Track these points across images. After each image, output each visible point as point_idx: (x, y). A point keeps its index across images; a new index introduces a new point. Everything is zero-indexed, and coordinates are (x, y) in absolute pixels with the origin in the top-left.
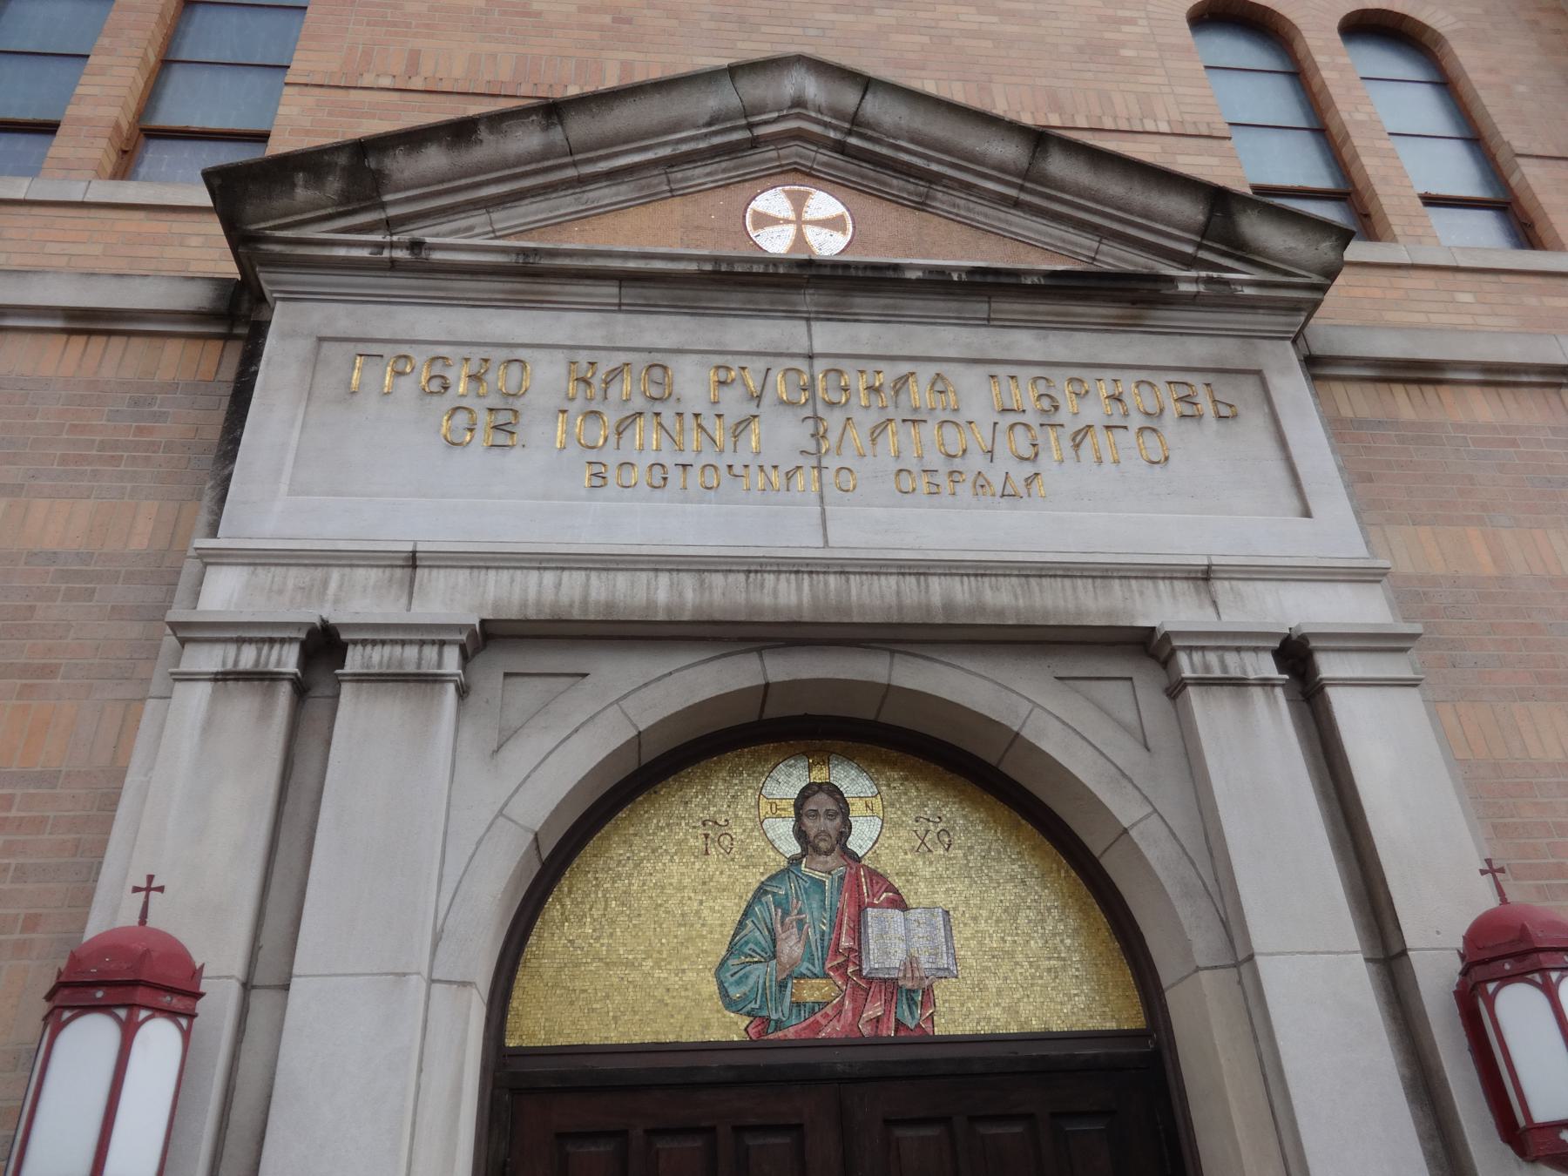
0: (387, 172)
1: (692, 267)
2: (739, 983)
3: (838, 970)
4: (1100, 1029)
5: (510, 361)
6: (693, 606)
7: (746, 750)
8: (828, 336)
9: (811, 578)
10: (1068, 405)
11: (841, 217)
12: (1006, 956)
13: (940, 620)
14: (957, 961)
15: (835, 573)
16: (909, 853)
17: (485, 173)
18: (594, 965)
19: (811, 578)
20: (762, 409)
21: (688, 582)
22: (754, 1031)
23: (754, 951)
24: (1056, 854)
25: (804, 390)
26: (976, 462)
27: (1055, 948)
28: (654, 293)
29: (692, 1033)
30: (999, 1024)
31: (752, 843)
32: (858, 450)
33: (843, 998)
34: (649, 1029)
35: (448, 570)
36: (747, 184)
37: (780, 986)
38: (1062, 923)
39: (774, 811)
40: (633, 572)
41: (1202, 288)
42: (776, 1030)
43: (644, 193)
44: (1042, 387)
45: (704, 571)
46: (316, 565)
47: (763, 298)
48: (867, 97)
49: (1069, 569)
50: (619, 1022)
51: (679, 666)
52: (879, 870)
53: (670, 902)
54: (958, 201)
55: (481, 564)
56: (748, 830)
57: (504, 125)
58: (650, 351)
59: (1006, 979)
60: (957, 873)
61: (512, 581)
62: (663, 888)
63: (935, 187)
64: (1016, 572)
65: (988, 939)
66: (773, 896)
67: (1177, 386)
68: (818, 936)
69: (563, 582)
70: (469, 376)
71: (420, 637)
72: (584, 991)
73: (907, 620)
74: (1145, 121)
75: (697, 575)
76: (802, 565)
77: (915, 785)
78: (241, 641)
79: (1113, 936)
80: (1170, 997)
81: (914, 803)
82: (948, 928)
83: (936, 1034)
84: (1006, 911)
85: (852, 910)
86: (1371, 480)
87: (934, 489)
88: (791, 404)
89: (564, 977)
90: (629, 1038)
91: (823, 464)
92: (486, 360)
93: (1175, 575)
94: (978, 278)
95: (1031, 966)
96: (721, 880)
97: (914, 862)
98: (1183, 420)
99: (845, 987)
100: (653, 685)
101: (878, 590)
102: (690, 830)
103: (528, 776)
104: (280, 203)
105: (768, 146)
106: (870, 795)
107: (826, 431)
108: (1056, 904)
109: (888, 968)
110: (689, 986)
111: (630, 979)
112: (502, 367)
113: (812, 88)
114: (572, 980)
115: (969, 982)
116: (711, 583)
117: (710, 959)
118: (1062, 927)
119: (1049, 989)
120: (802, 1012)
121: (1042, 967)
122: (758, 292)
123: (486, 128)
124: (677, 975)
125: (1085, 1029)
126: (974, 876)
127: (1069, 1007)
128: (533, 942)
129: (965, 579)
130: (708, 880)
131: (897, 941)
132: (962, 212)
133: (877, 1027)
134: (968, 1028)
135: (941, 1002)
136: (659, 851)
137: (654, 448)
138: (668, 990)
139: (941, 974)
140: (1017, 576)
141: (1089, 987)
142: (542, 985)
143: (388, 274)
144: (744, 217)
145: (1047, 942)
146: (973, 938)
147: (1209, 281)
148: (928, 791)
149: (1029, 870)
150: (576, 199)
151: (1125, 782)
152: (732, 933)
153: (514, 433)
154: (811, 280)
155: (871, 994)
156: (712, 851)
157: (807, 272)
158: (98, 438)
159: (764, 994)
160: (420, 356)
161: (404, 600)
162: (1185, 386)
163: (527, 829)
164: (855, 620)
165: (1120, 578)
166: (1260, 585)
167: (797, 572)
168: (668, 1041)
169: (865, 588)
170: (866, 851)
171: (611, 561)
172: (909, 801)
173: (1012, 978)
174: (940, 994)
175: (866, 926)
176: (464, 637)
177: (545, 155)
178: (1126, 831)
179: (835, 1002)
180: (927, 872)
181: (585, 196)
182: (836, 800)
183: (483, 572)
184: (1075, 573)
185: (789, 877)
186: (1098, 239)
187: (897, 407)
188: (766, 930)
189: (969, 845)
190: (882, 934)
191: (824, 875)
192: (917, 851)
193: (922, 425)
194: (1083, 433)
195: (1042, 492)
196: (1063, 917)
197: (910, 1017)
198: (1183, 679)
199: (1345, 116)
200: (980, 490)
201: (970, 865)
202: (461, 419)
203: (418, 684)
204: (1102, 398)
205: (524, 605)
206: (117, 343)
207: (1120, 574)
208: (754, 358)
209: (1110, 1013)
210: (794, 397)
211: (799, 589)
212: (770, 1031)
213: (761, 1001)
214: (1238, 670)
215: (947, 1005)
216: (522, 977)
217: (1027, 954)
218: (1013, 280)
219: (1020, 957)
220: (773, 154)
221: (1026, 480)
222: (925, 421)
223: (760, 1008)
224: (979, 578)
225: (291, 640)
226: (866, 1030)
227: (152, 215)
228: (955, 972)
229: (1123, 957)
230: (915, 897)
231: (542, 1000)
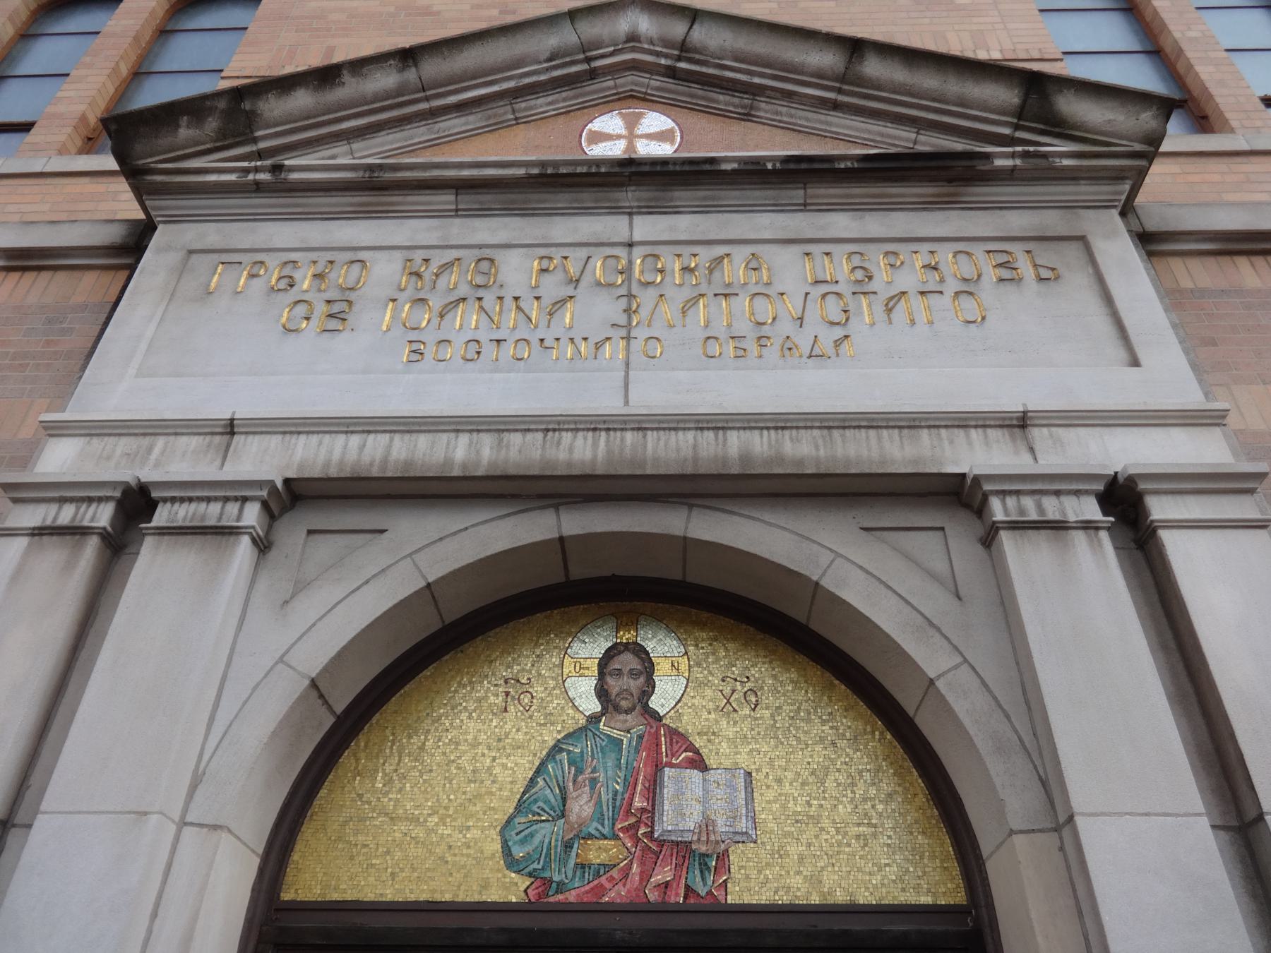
0: (259, 112)
1: (521, 172)
2: (523, 842)
3: (628, 831)
4: (913, 903)
5: (352, 262)
6: (489, 462)
7: (556, 612)
8: (647, 227)
9: (608, 435)
10: (882, 275)
11: (671, 131)
12: (811, 821)
13: (735, 470)
14: (757, 824)
15: (633, 429)
16: (713, 712)
17: (345, 110)
18: (380, 819)
19: (608, 435)
20: (578, 290)
21: (487, 440)
22: (534, 892)
23: (543, 810)
24: (871, 716)
25: (621, 273)
26: (786, 327)
27: (866, 814)
28: (487, 198)
29: (470, 893)
30: (799, 894)
31: (552, 701)
32: (669, 321)
33: (631, 861)
34: (425, 887)
35: (263, 436)
36: (586, 111)
37: (566, 847)
38: (874, 788)
39: (577, 670)
40: (435, 434)
41: (1018, 162)
42: (557, 892)
43: (491, 121)
44: (856, 261)
45: (503, 431)
46: (144, 435)
47: (587, 197)
48: (695, 27)
49: (873, 420)
50: (397, 879)
51: (476, 522)
52: (680, 730)
53: (463, 758)
54: (780, 109)
55: (293, 429)
56: (549, 689)
57: (365, 70)
58: (480, 247)
59: (809, 845)
60: (763, 733)
61: (320, 443)
62: (457, 744)
63: (758, 98)
64: (817, 424)
65: (792, 802)
66: (568, 754)
67: (995, 254)
68: (610, 795)
69: (368, 444)
70: (315, 276)
71: (222, 494)
72: (365, 846)
73: (702, 471)
74: (977, 51)
75: (496, 435)
76: (599, 422)
77: (724, 645)
78: (63, 500)
79: (931, 803)
80: (991, 867)
81: (722, 663)
82: (749, 789)
83: (729, 902)
84: (813, 773)
85: (649, 769)
86: (1215, 345)
87: (742, 353)
88: (611, 285)
89: (348, 831)
90: (404, 896)
91: (632, 335)
92: (331, 262)
93: (988, 423)
94: (792, 166)
95: (838, 832)
96: (517, 737)
97: (717, 722)
98: (1001, 284)
99: (634, 849)
100: (448, 539)
101: (674, 444)
102: (492, 688)
103: (314, 625)
104: (164, 141)
105: (605, 77)
106: (677, 655)
107: (638, 306)
108: (868, 767)
109: (682, 831)
110: (472, 844)
111: (413, 835)
112: (346, 267)
114: (356, 834)
115: (768, 847)
116: (509, 442)
117: (496, 817)
118: (874, 792)
119: (857, 857)
120: (587, 874)
121: (850, 834)
122: (582, 192)
123: (349, 72)
124: (461, 832)
125: (896, 903)
126: (780, 736)
127: (879, 877)
128: (323, 795)
129: (765, 432)
130: (503, 737)
131: (694, 802)
132: (785, 119)
133: (665, 893)
134: (764, 898)
135: (737, 868)
136: (459, 708)
137: (473, 327)
138: (450, 847)
139: (738, 838)
140: (819, 428)
141: (902, 857)
142: (325, 838)
143: (253, 195)
144: (581, 136)
145: (856, 807)
146: (775, 802)
147: (1026, 155)
148: (738, 651)
149: (841, 731)
150: (428, 129)
151: (932, 632)
152: (522, 790)
153: (345, 320)
154: (633, 178)
155: (661, 857)
156: (511, 708)
157: (627, 170)
158: (12, 350)
159: (548, 854)
160: (273, 261)
161: (218, 462)
162: (1005, 254)
163: (303, 675)
164: (649, 472)
165: (929, 427)
166: (1082, 431)
167: (595, 429)
168: (443, 900)
169: (662, 443)
170: (668, 710)
171: (413, 424)
172: (717, 661)
173: (817, 845)
174: (736, 860)
175: (662, 787)
176: (264, 493)
177: (399, 92)
178: (932, 682)
179: (622, 865)
180: (731, 732)
181: (437, 126)
182: (639, 657)
183: (295, 436)
184: (880, 424)
185: (586, 735)
186: (916, 130)
187: (710, 283)
188: (557, 788)
189: (777, 705)
190: (679, 793)
191: (622, 733)
192: (722, 710)
193: (733, 299)
194: (896, 298)
195: (852, 352)
196: (877, 780)
197: (701, 883)
198: (994, 523)
199: (1177, 35)
200: (787, 353)
201: (778, 725)
202: (301, 310)
203: (215, 536)
204: (918, 268)
205: (327, 464)
206: (45, 275)
207: (928, 424)
208: (577, 249)
209: (926, 886)
210: (611, 280)
211: (595, 444)
212: (550, 893)
213: (545, 862)
214: (1057, 513)
215: (743, 871)
216: (307, 831)
217: (834, 820)
218: (826, 166)
219: (826, 823)
220: (611, 83)
221: (836, 341)
222: (737, 295)
223: (543, 869)
224: (780, 431)
225: (108, 499)
226: (653, 896)
227: (95, 180)
228: (754, 836)
229: (942, 825)
230: (716, 757)
231: (323, 854)
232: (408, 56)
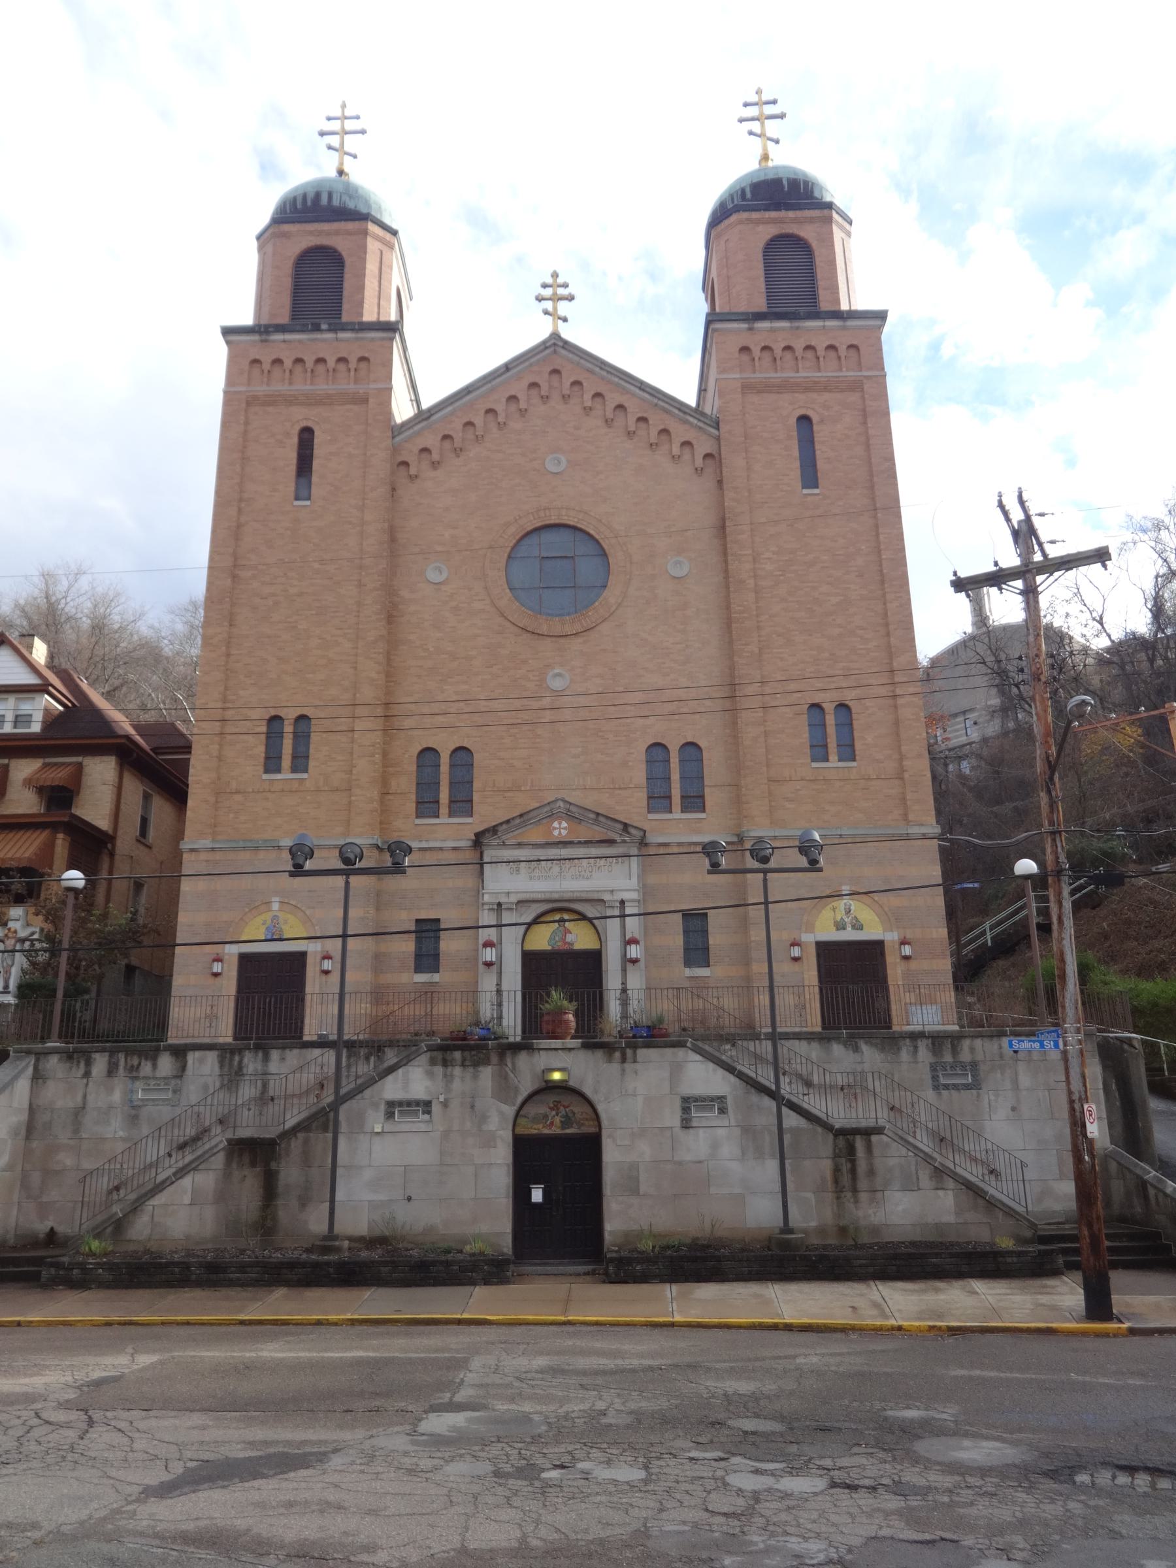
26: (583, 873)
113: (561, 804)
232: (521, 816)
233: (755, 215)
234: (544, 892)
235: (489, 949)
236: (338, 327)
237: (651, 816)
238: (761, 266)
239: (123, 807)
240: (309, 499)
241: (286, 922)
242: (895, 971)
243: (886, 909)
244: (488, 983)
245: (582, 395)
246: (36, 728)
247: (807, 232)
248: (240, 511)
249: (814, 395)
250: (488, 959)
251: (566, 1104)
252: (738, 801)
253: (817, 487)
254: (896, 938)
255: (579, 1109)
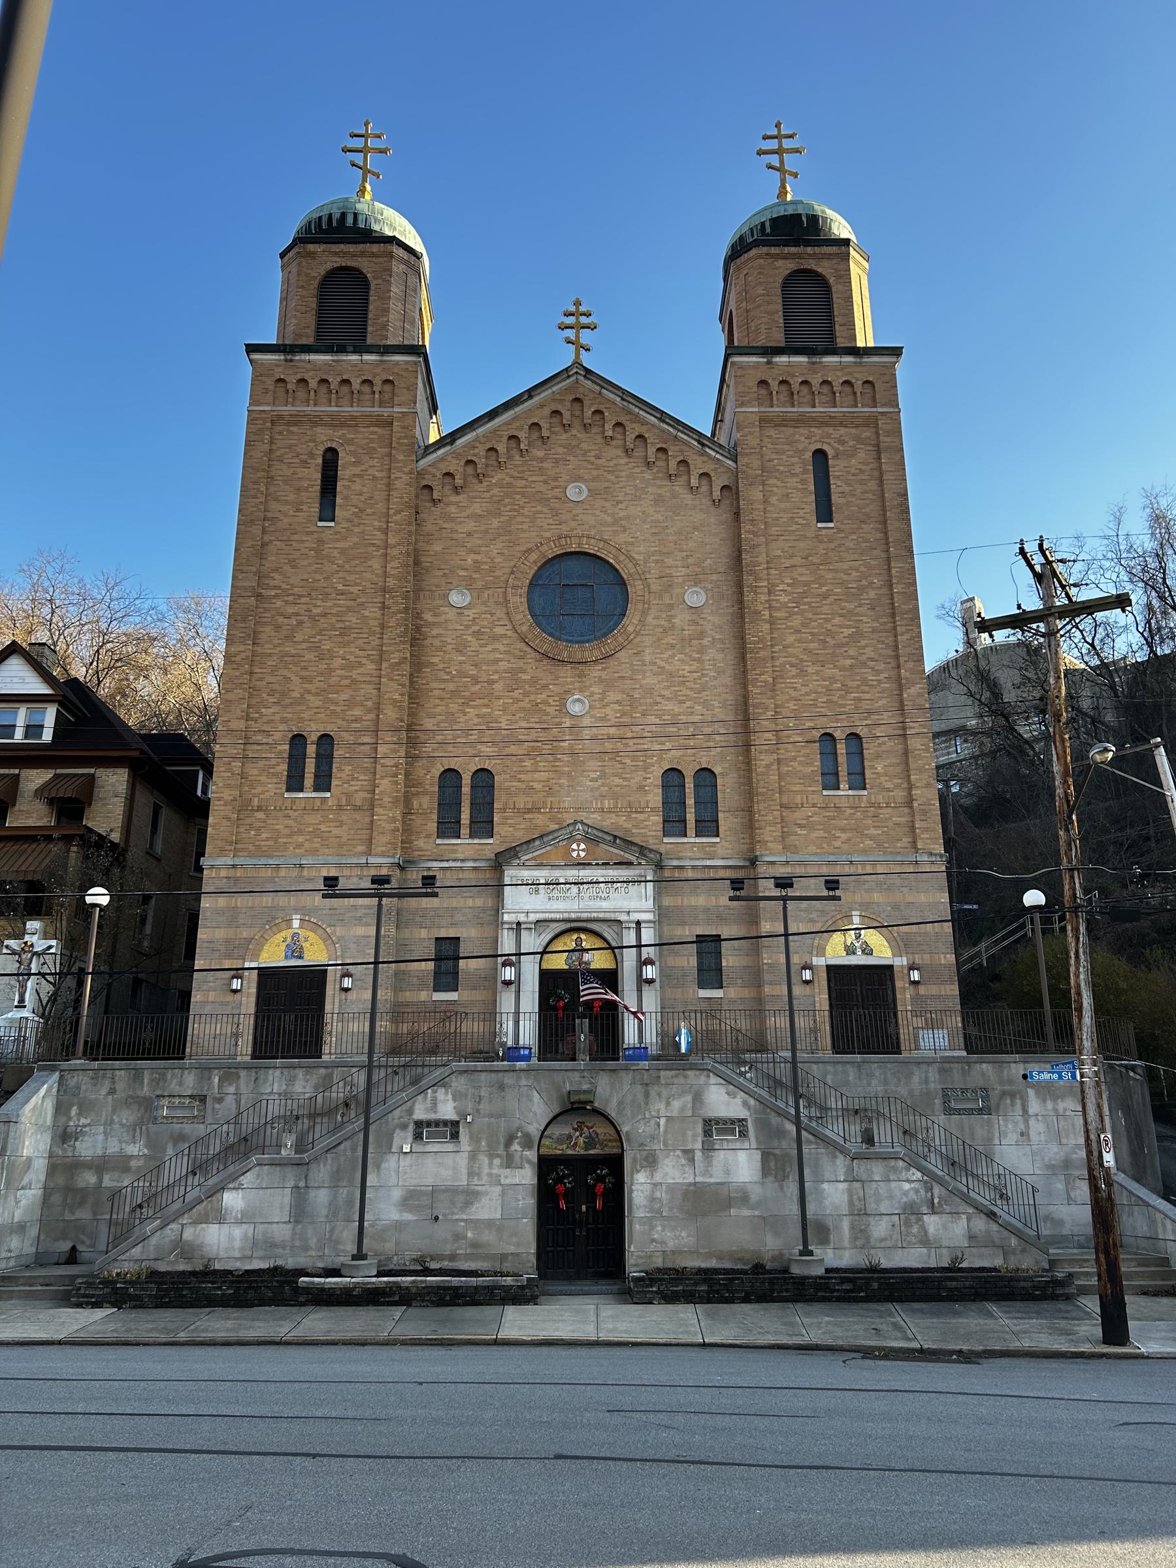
26: (601, 894)
113: (579, 826)
232: (541, 837)
233: (774, 250)
234: (562, 912)
235: (508, 968)
236: (361, 348)
237: (666, 840)
238: (780, 301)
239: (135, 819)
240: (333, 520)
241: (306, 940)
242: (905, 997)
243: (896, 935)
244: (506, 1002)
245: (603, 426)
246: (47, 736)
247: (824, 268)
248: (264, 531)
249: (831, 430)
250: (508, 978)
251: (590, 1125)
252: (750, 826)
253: (831, 521)
254: (905, 963)
255: (602, 1130)
